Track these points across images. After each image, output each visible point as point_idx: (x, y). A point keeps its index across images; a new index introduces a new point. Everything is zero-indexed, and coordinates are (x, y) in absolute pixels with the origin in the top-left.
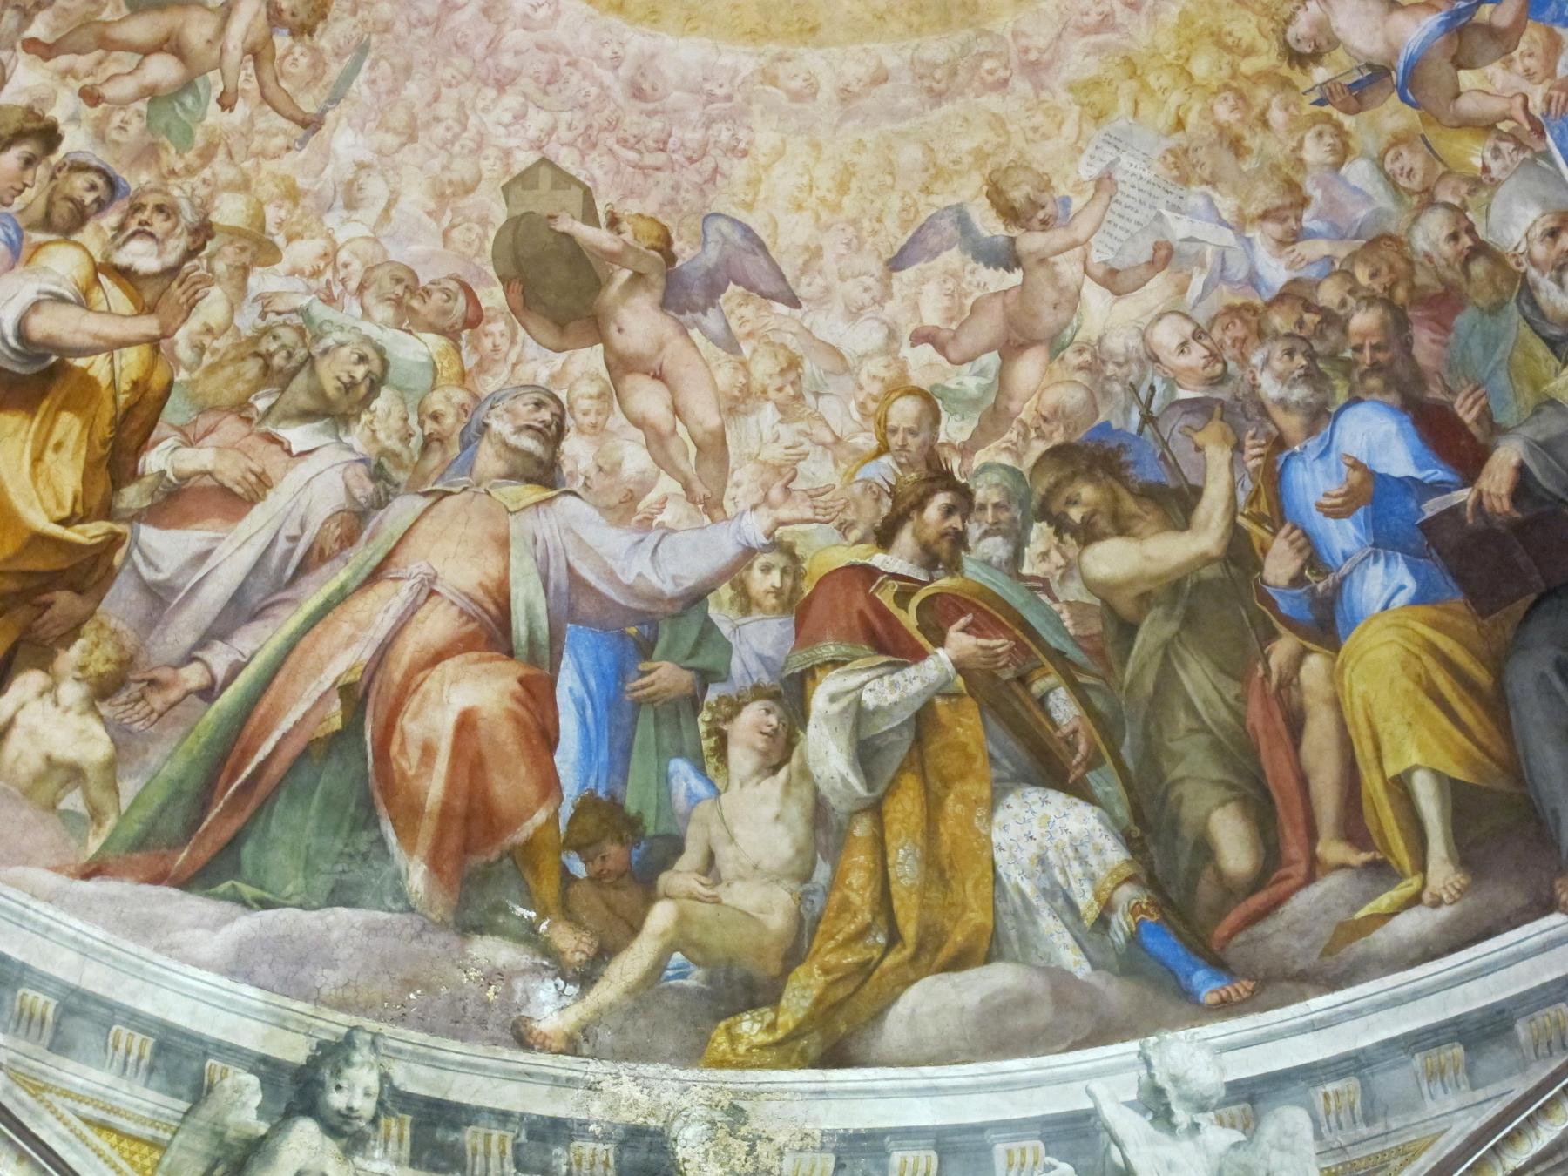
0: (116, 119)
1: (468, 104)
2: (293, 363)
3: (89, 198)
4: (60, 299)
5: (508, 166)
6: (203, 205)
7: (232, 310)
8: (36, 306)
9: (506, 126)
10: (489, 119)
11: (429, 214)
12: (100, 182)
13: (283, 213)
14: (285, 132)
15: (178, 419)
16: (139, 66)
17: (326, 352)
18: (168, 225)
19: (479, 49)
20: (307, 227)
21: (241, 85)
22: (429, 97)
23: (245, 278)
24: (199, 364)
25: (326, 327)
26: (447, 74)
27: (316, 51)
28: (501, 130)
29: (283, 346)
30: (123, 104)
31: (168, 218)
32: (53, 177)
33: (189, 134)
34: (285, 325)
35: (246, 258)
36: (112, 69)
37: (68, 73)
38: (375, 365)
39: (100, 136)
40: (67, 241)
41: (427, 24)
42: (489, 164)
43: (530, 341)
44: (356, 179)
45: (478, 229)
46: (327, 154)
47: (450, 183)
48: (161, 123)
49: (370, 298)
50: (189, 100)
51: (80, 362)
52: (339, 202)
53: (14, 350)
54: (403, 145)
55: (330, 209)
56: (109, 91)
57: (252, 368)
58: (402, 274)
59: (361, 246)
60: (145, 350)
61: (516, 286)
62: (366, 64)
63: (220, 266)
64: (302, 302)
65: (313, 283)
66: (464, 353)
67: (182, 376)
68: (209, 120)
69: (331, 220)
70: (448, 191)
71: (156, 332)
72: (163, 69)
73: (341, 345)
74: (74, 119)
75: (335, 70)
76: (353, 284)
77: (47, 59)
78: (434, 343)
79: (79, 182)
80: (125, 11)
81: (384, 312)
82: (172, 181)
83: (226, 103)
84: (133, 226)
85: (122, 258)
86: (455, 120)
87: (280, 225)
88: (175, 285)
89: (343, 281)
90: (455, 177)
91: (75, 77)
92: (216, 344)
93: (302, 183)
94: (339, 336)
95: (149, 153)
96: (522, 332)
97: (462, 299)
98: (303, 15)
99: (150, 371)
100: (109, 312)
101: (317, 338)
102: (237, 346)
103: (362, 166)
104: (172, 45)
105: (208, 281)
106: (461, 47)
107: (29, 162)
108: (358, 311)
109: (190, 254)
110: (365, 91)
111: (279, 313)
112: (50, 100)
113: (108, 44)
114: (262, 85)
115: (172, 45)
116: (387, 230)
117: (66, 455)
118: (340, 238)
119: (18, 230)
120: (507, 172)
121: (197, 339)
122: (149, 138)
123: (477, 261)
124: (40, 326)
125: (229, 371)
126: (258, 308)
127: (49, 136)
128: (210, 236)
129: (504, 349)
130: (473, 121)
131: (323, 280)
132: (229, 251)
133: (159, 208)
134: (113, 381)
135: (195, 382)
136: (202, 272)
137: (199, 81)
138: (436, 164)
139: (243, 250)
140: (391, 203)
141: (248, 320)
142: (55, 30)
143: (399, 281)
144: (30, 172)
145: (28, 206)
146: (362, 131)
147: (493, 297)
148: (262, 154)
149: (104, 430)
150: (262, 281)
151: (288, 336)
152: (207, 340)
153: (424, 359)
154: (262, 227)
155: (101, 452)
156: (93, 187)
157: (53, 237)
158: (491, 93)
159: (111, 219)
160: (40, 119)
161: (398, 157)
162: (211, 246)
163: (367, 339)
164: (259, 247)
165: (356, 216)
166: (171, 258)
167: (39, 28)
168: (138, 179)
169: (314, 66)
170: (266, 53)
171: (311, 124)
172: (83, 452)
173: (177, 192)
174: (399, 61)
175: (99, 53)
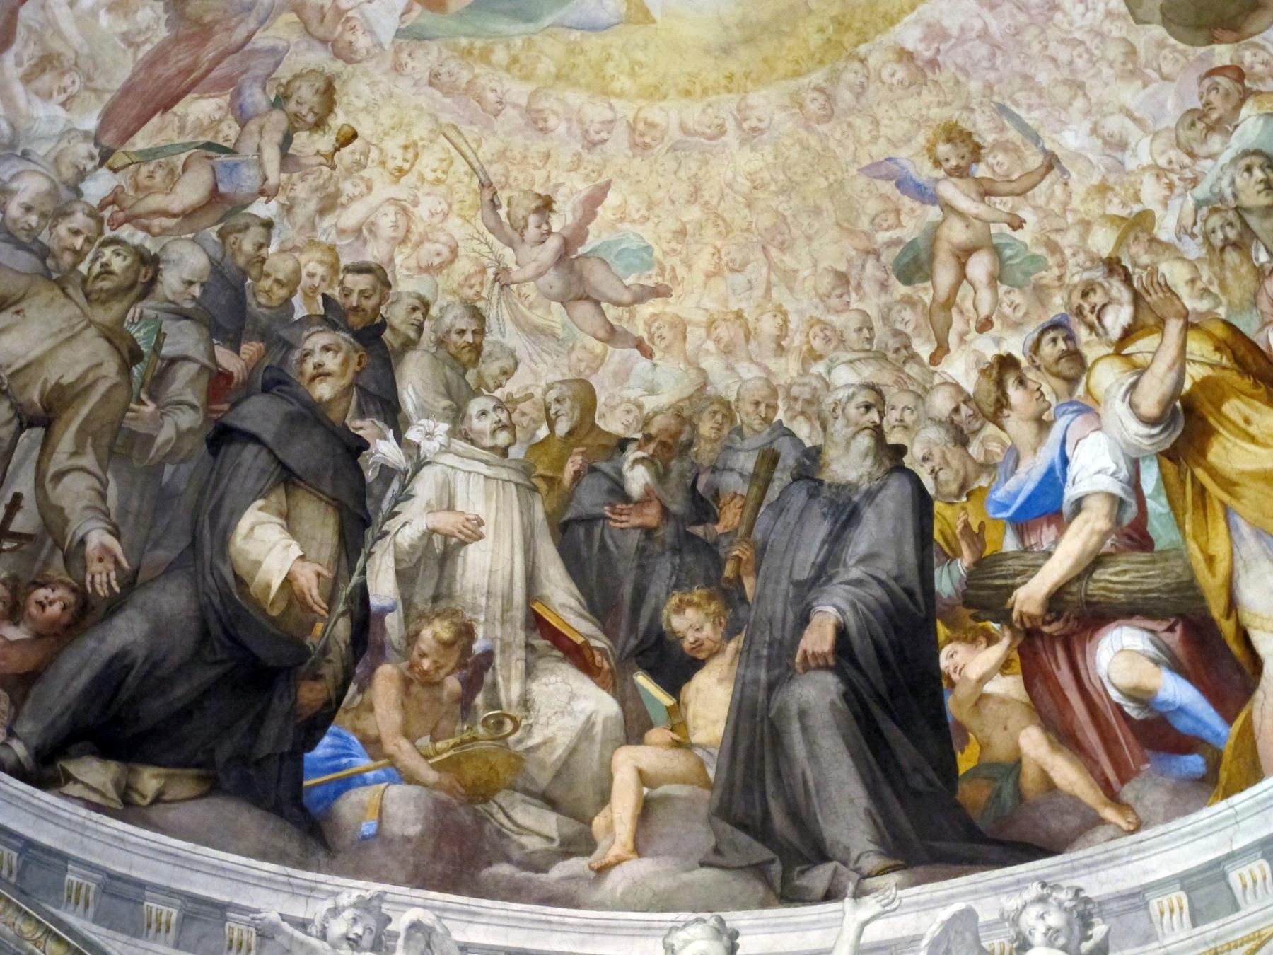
0: (1007, 310)
1: (1063, 35)
2: (1238, 224)
3: (1062, 345)
4: (1133, 386)
5: (1119, 16)
6: (1092, 260)
7: (1181, 259)
8: (1132, 406)
9: (1087, 9)
10: (1079, 22)
11: (1145, 86)
12: (1052, 334)
13: (1116, 201)
14: (1052, 184)
15: (1256, 324)
16: (972, 284)
17: (1235, 196)
18: (1099, 291)
19: (1022, 18)
20: (1132, 184)
21: (1006, 210)
22: (1051, 66)
23: (1159, 242)
24: (1216, 296)
25: (1216, 190)
26: (1036, 47)
27: (996, 146)
28: (1090, 14)
29: (1222, 227)
30: (997, 302)
31: (1094, 290)
32: (1038, 368)
33: (1034, 258)
34: (1205, 222)
35: (1144, 237)
36: (968, 305)
37: (962, 339)
38: (1257, 161)
39: (1017, 325)
40: (1090, 370)
41: (994, 55)
42: (1117, 30)
43: (1265, 34)
44: (1103, 138)
45: (1166, 52)
46: (1077, 155)
47: (1124, 64)
48: (1018, 275)
49: (1200, 150)
50: (1008, 252)
51: (1187, 385)
52: (1119, 155)
53: (1162, 432)
54: (1085, 95)
55: (1122, 163)
56: (984, 310)
57: (1232, 257)
58: (1188, 120)
59: (1158, 145)
60: (1192, 335)
61: (1218, 33)
62: (1014, 109)
63: (1145, 259)
64: (1190, 203)
65: (1177, 191)
66: (1263, 89)
67: (1222, 312)
68: (1028, 241)
69: (1131, 164)
70: (1130, 66)
71: (1181, 323)
72: (979, 267)
73: (1233, 182)
74: (998, 341)
75: (1013, 134)
76: (1187, 160)
77: (948, 350)
78: (1249, 110)
79: (1047, 350)
80: (929, 284)
81: (1215, 142)
82: (1067, 280)
83: (1017, 224)
84: (1092, 318)
85: (1115, 333)
86: (1074, 48)
87: (1124, 204)
88: (1148, 299)
89: (1183, 167)
90: (1121, 59)
91: (967, 333)
92: (1205, 278)
93: (1095, 180)
94: (1225, 182)
95: (1040, 293)
96: (1256, 39)
97: (1219, 79)
98: (965, 150)
99: (1210, 335)
100: (1154, 353)
101: (1222, 199)
102: (1211, 264)
103: (1094, 131)
104: (963, 255)
105: (1153, 271)
106: (1018, 31)
107: (1022, 382)
108: (1209, 163)
109: (1127, 280)
110: (1036, 114)
111: (1195, 223)
112: (979, 357)
113: (949, 304)
114: (1012, 194)
115: (963, 255)
116: (1150, 122)
117: (1255, 417)
118: (1146, 160)
119: (1071, 403)
120: (1124, 17)
121: (1196, 292)
122: (1028, 289)
123: (1191, 58)
124: (1150, 406)
125: (1229, 274)
126: (1187, 238)
127: (1006, 363)
128: (1119, 261)
129: (1267, 56)
130: (1078, 35)
131: (1177, 182)
132: (1134, 250)
133: (1085, 295)
134: (1212, 366)
135: (1230, 303)
136: (1144, 275)
137: (995, 241)
138: (1107, 72)
139: (1136, 238)
140: (1129, 115)
141: (1193, 249)
142: (928, 339)
143: (1193, 124)
144: (1030, 384)
145: (1054, 391)
146: (1064, 123)
147: (1223, 53)
148: (1065, 206)
149: (1246, 383)
150: (1166, 229)
151: (1215, 221)
152: (1199, 285)
153: (1261, 122)
154: (1123, 219)
155: (1262, 390)
156: (1054, 340)
157: (1084, 379)
158: (1058, 16)
159: (1083, 333)
160: (991, 366)
161: (1094, 100)
162: (1126, 262)
163: (1234, 161)
164: (1138, 225)
165: (1133, 144)
166: (1126, 296)
167: (924, 350)
168: (1057, 305)
169: (1006, 150)
170: (987, 186)
171: (1051, 163)
172: (1258, 404)
173: (1076, 278)
174: (1017, 83)
175: (954, 311)
